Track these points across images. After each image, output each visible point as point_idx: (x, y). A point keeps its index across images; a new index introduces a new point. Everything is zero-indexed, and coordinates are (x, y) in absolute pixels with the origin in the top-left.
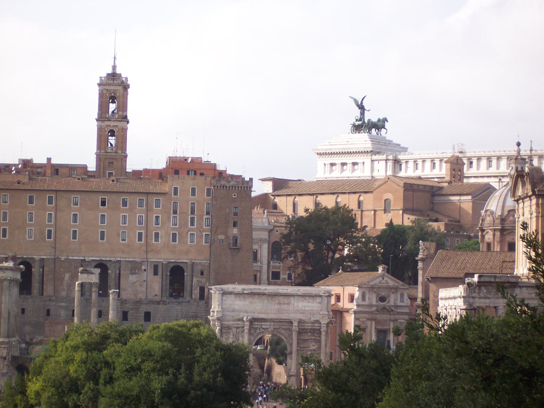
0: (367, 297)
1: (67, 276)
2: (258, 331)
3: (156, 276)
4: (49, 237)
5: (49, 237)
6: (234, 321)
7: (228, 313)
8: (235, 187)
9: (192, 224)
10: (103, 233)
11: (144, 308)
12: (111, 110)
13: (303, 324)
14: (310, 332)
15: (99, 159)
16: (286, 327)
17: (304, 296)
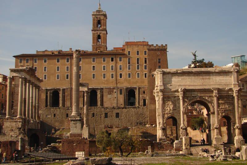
3: (121, 95)
8: (159, 49)
9: (138, 68)
10: (94, 75)
13: (221, 92)
14: (226, 98)
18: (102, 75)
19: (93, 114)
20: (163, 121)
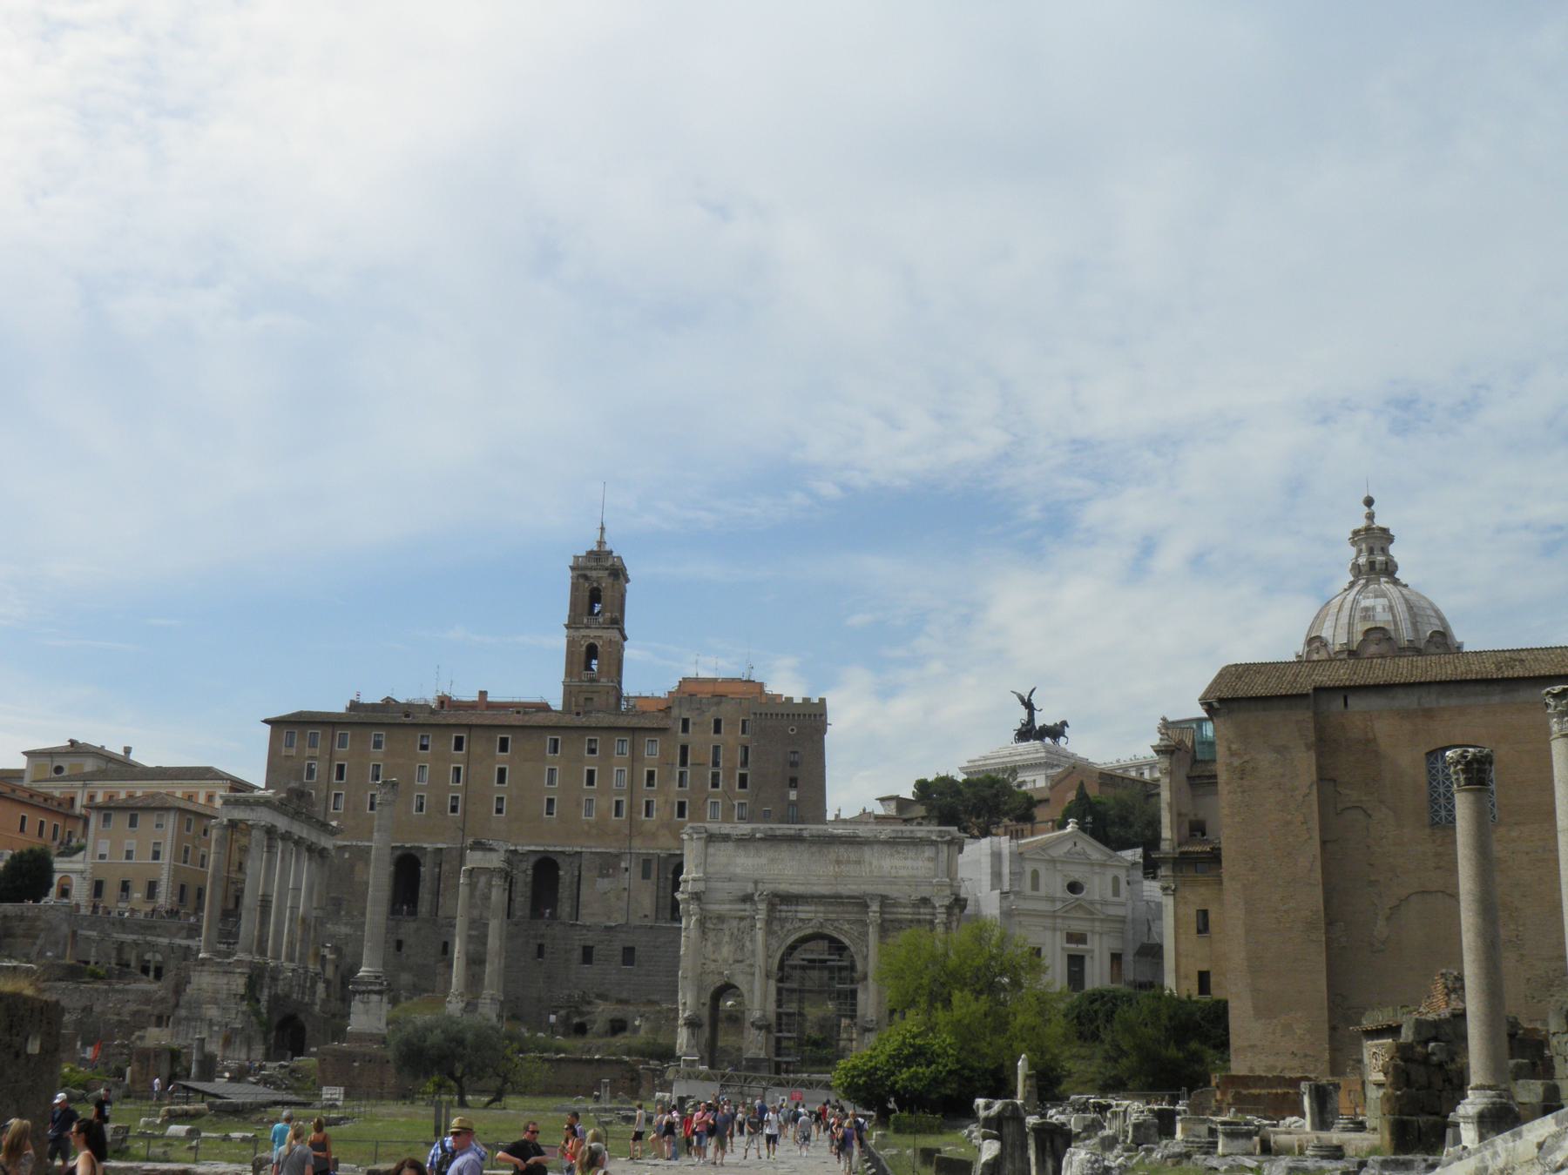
0: (1042, 881)
2: (788, 926)
4: (454, 809)
5: (454, 809)
6: (731, 902)
7: (719, 885)
9: (715, 785)
10: (551, 802)
16: (852, 917)
18: (579, 805)
19: (541, 948)
20: (698, 997)
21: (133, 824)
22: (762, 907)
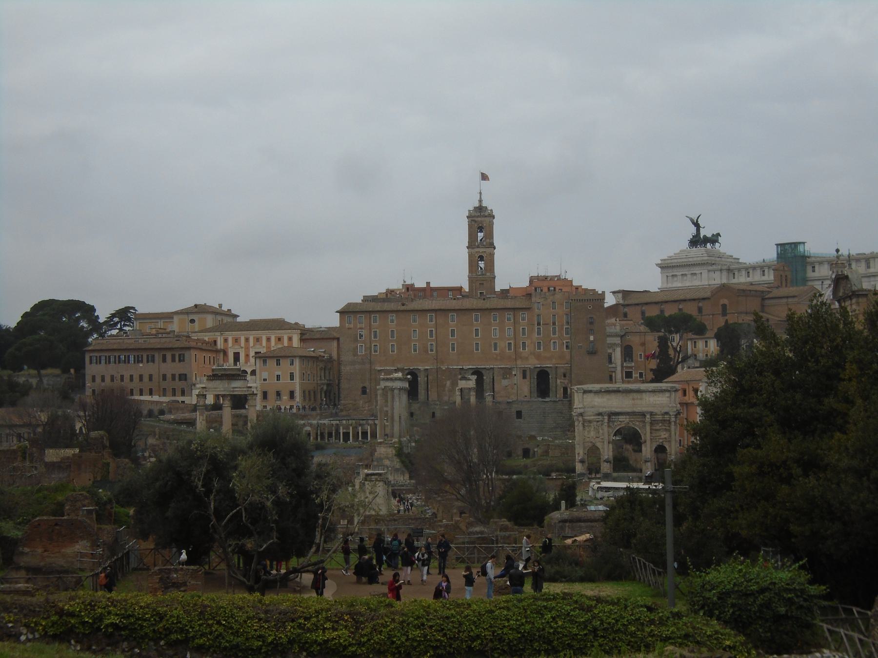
1: (448, 383)
9: (554, 333)
11: (515, 408)
12: (479, 239)
15: (471, 280)
17: (654, 391)
21: (278, 364)
22: (606, 417)
